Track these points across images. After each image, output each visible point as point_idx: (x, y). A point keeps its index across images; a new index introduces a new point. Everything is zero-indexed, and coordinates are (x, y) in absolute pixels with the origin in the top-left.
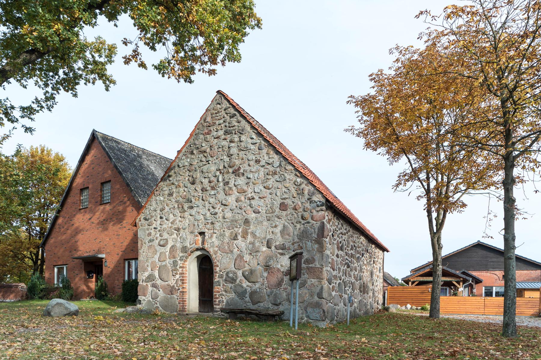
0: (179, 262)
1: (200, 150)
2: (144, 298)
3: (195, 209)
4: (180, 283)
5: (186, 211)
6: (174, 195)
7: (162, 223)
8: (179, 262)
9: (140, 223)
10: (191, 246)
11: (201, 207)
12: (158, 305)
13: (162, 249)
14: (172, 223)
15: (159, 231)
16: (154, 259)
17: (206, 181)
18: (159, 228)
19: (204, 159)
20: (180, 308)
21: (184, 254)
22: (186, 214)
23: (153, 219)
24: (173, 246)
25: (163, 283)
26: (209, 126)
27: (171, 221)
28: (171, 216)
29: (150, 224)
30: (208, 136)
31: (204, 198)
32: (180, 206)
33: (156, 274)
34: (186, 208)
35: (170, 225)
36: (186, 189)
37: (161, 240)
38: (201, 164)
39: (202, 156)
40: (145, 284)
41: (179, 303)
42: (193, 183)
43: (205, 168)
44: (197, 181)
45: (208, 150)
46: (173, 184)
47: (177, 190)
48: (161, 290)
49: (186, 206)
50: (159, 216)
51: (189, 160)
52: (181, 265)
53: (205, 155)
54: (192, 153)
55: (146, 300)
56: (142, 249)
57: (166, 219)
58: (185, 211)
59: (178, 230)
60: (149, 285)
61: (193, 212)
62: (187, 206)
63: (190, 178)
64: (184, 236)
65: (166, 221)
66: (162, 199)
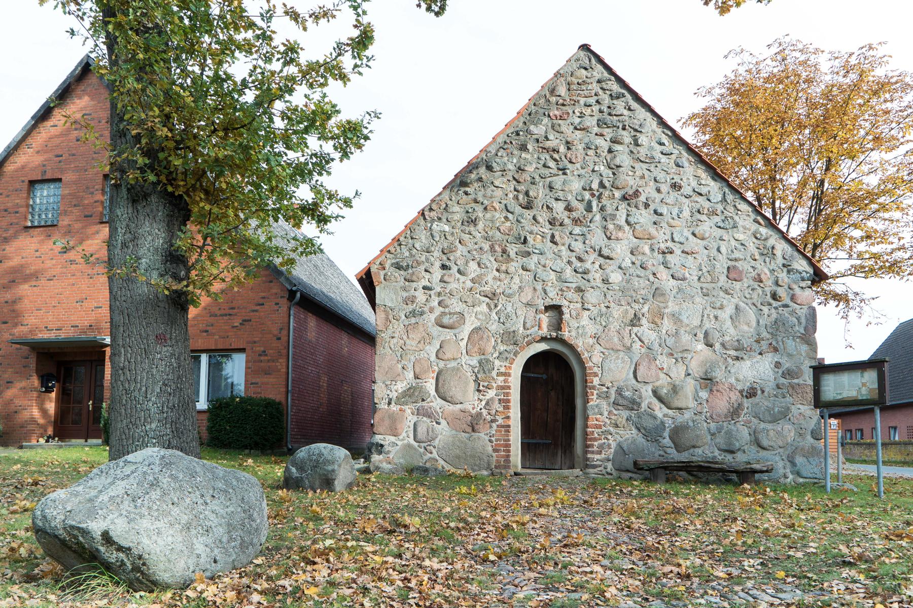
0: (497, 363)
1: (541, 145)
2: (393, 439)
3: (535, 258)
4: (497, 406)
5: (513, 260)
6: (481, 225)
7: (446, 278)
8: (497, 363)
9: (382, 273)
10: (529, 332)
11: (550, 255)
12: (435, 455)
13: (448, 334)
14: (473, 281)
15: (439, 294)
16: (423, 355)
17: (559, 207)
18: (438, 289)
19: (552, 164)
20: (497, 461)
21: (511, 347)
22: (513, 267)
23: (423, 268)
24: (477, 330)
25: (450, 408)
26: (563, 105)
27: (473, 275)
28: (473, 265)
29: (414, 278)
30: (560, 122)
31: (557, 238)
32: (497, 248)
33: (430, 386)
34: (512, 254)
35: (469, 284)
36: (510, 216)
37: (443, 314)
38: (546, 172)
39: (548, 157)
40: (394, 408)
41: (495, 450)
42: (528, 206)
43: (558, 181)
44: (539, 203)
45: (562, 149)
46: (476, 201)
47: (488, 215)
48: (444, 422)
49: (512, 250)
50: (438, 264)
51: (515, 161)
52: (503, 370)
53: (556, 156)
54: (523, 148)
55: (400, 443)
56: (389, 332)
57: (459, 272)
58: (509, 259)
59: (492, 296)
60: (409, 411)
61: (532, 262)
62: (515, 250)
63: (521, 197)
64: (509, 309)
65: (458, 275)
66: (447, 228)
